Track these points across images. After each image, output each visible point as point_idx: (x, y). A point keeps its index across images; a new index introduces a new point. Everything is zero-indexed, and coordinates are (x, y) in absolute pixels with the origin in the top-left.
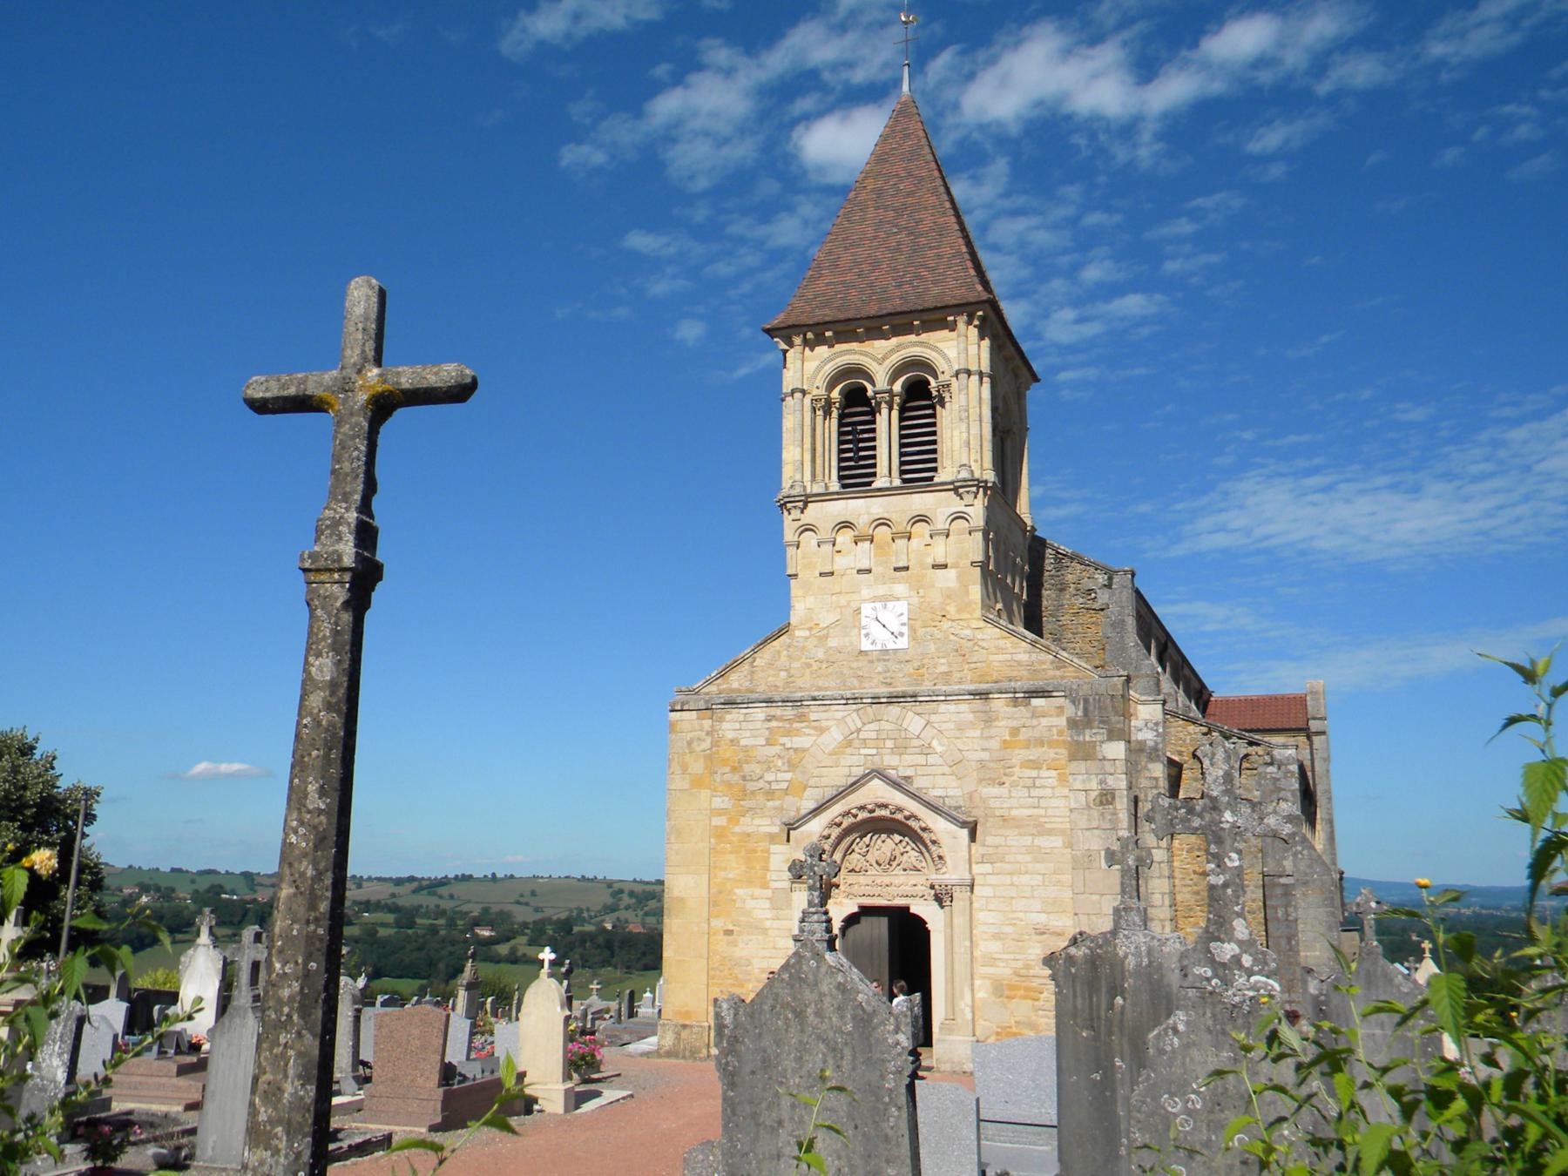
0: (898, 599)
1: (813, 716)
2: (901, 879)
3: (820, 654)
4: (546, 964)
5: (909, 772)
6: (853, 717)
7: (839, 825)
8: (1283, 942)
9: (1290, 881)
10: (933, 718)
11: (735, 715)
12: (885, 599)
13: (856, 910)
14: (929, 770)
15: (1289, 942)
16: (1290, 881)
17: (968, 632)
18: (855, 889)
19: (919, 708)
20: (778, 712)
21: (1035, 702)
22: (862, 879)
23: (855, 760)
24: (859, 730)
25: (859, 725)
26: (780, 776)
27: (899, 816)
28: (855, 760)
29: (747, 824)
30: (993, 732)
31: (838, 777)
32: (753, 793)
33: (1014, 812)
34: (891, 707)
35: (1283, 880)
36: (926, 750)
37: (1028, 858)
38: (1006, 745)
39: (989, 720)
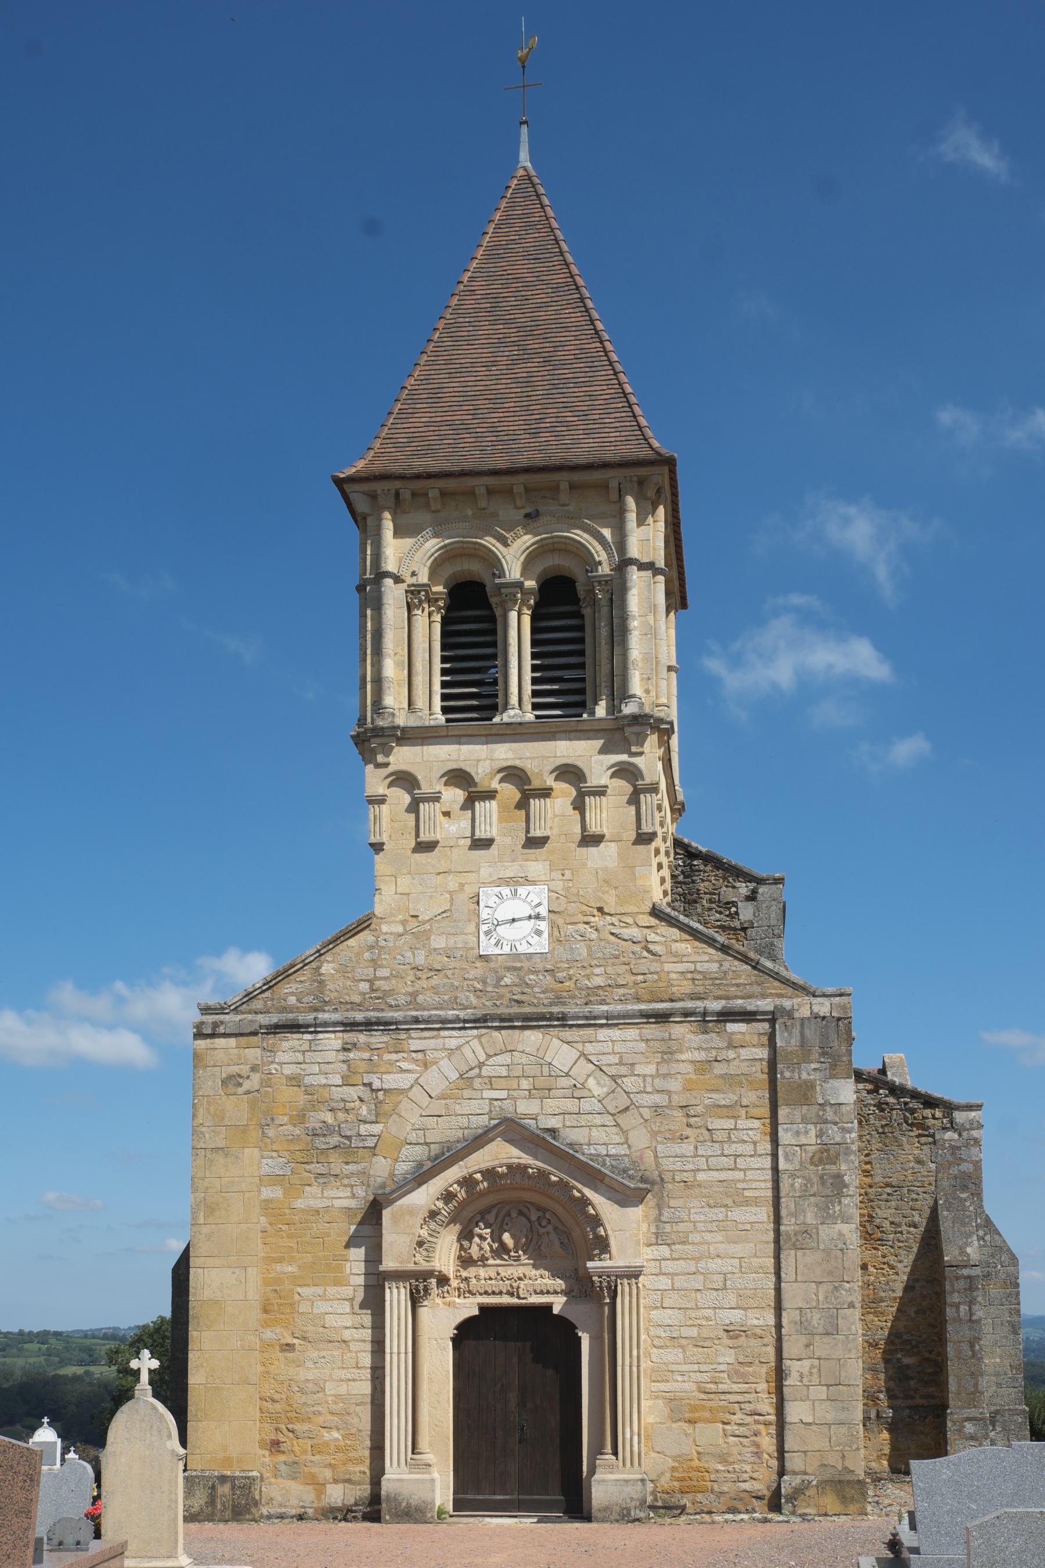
0: (533, 883)
1: (415, 1045)
3: (421, 959)
4: (145, 1377)
5: (553, 1123)
6: (473, 1045)
8: (965, 1347)
9: (977, 1271)
10: (589, 1048)
11: (294, 1041)
12: (513, 882)
13: (476, 1312)
14: (583, 1120)
15: (972, 1346)
16: (977, 1271)
17: (634, 932)
19: (568, 1034)
20: (362, 1038)
21: (731, 1027)
22: (482, 1272)
23: (474, 1106)
24: (481, 1065)
25: (482, 1057)
26: (364, 1129)
28: (474, 1106)
29: (313, 1197)
30: (675, 1067)
31: (447, 1130)
32: (324, 1152)
33: (701, 1176)
34: (527, 1033)
35: (965, 1272)
36: (577, 1091)
37: (719, 1237)
38: (688, 1088)
39: (668, 1053)
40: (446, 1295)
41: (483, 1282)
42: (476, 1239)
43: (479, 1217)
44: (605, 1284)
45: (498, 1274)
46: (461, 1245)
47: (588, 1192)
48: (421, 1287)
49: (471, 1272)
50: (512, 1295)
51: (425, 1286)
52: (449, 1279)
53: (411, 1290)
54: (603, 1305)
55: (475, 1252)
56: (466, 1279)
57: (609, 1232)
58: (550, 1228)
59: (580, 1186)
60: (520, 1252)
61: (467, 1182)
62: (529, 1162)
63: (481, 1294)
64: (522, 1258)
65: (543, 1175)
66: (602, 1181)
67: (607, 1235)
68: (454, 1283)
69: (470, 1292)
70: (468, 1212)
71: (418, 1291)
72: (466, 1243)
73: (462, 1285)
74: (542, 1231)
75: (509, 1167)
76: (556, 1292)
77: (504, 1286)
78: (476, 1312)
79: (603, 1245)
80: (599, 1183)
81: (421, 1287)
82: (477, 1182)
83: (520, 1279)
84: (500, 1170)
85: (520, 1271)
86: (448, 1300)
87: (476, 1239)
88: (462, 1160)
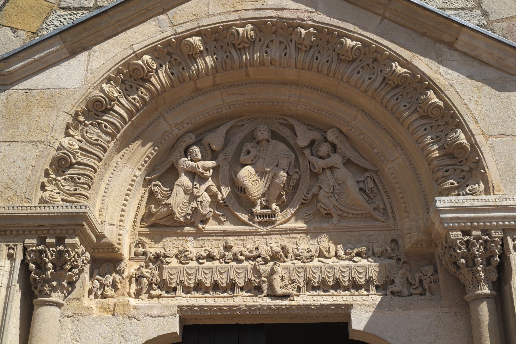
41: (194, 263)
42: (184, 180)
43: (191, 138)
44: (478, 249)
45: (228, 248)
46: (152, 193)
47: (425, 65)
49: (170, 245)
50: (257, 290)
51: (60, 254)
52: (119, 260)
53: (24, 264)
54: (466, 307)
55: (178, 201)
56: (158, 259)
57: (479, 139)
58: (336, 159)
59: (406, 54)
60: (274, 206)
61: (172, 52)
62: (301, 15)
64: (280, 218)
65: (328, 37)
66: (451, 45)
67: (474, 145)
69: (164, 285)
70: (173, 123)
71: (41, 267)
72: (158, 188)
74: (320, 163)
75: (260, 25)
76: (355, 286)
77: (242, 271)
78: (173, 326)
79: (465, 166)
80: (446, 49)
81: (49, 256)
82: (193, 55)
84: (240, 30)
85: (275, 243)
87: (184, 180)
88: (164, 11)
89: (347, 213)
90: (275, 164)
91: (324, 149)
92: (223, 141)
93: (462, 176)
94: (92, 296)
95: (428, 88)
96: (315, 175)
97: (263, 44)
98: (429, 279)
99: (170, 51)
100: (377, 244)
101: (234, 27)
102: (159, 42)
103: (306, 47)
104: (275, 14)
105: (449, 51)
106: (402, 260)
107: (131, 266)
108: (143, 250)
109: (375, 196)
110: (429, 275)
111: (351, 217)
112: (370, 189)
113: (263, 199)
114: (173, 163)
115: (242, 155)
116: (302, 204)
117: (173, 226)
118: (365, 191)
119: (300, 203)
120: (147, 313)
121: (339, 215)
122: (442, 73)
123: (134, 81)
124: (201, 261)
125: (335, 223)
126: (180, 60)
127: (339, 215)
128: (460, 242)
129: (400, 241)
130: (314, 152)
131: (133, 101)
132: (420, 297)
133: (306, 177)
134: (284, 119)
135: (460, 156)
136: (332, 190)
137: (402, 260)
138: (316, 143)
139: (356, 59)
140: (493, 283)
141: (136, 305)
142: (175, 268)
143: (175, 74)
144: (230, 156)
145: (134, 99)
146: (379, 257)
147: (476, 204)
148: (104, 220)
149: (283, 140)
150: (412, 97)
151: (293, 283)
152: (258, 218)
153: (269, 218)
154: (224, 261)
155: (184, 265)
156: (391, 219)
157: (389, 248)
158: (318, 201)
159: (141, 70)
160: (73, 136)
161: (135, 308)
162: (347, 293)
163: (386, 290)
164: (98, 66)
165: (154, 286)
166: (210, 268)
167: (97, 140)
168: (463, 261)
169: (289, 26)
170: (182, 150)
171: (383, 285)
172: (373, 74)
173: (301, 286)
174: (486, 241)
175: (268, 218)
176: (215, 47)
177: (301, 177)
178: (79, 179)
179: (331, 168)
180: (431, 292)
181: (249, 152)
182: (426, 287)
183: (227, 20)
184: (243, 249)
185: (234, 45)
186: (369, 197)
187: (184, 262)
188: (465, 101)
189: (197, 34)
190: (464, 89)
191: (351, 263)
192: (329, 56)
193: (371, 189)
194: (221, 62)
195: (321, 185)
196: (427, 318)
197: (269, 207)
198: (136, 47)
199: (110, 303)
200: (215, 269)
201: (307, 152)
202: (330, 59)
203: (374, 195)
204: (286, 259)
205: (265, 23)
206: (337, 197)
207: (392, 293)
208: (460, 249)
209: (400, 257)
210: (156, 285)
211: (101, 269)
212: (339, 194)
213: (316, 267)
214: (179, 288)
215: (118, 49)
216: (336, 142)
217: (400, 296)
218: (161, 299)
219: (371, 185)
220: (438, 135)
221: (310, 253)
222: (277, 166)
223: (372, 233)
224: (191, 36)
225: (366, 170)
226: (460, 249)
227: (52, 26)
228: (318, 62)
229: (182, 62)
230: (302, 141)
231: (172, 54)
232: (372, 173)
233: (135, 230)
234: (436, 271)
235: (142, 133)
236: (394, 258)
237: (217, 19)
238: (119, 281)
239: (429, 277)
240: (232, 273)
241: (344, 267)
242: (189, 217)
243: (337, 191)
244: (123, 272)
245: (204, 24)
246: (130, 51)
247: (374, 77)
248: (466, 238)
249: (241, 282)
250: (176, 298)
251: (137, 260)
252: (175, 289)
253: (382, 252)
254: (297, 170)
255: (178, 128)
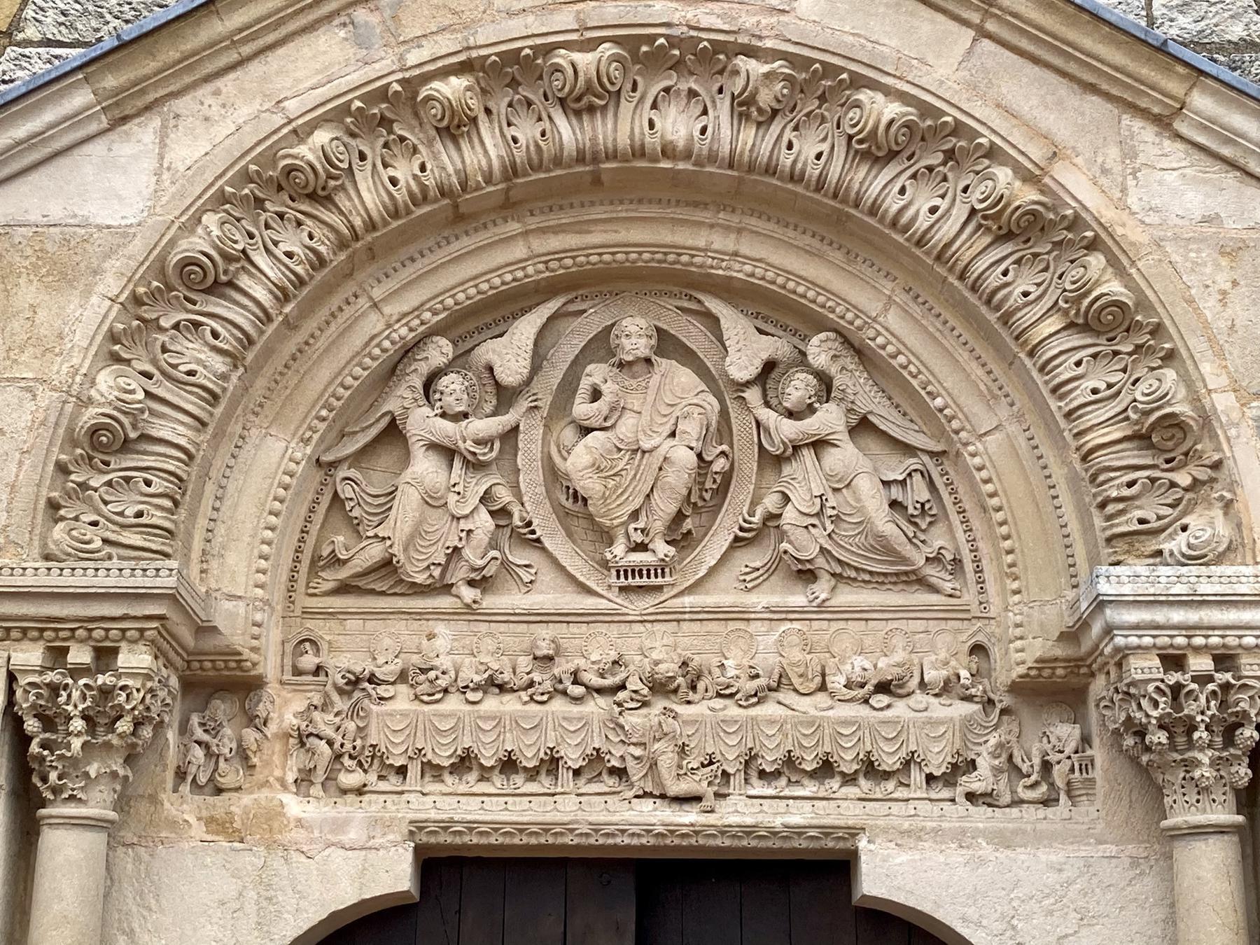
2: (767, 648)
7: (318, 191)
13: (395, 875)
18: (395, 717)
22: (447, 645)
27: (808, 148)
40: (230, 775)
44: (1200, 707)
48: (75, 702)
58: (829, 419)
63: (432, 770)
66: (1163, 123)
68: (285, 708)
73: (324, 723)
74: (788, 429)
80: (1146, 133)
83: (661, 687)
86: (240, 804)
89: (857, 569)
90: (667, 430)
91: (798, 388)
92: (527, 363)
93: (1169, 501)
94: (185, 788)
95: (1093, 245)
96: (774, 461)
97: (642, 99)
98: (1069, 762)
99: (388, 114)
100: (933, 658)
101: (563, 51)
102: (358, 93)
103: (760, 110)
104: (677, 15)
105: (1157, 140)
106: (999, 706)
107: (286, 702)
108: (317, 660)
109: (931, 523)
110: (1068, 751)
111: (864, 581)
112: (918, 506)
113: (633, 526)
114: (394, 420)
115: (577, 401)
116: (737, 539)
117: (395, 594)
118: (906, 508)
119: (732, 537)
120: (333, 839)
121: (834, 575)
122: (1135, 208)
123: (290, 202)
124: (471, 696)
125: (823, 596)
126: (416, 142)
127: (834, 575)
128: (1157, 688)
129: (996, 652)
130: (771, 394)
131: (286, 260)
132: (1042, 812)
133: (748, 463)
134: (691, 298)
135: (1170, 444)
136: (817, 508)
137: (999, 706)
138: (777, 370)
139: (898, 152)
140: (1237, 792)
141: (303, 815)
142: (404, 714)
143: (402, 183)
144: (546, 402)
145: (290, 255)
146: (936, 695)
147: (1205, 588)
148: (213, 586)
149: (687, 356)
150: (1046, 269)
151: (711, 763)
152: (618, 577)
153: (649, 577)
154: (532, 699)
155: (426, 708)
156: (973, 588)
157: (964, 674)
158: (782, 536)
159: (311, 176)
160: (128, 362)
161: (300, 823)
162: (851, 791)
163: (954, 785)
164: (188, 163)
165: (346, 761)
166: (494, 718)
167: (191, 373)
168: (1162, 737)
169: (718, 47)
170: (418, 383)
171: (944, 773)
172: (943, 197)
173: (731, 771)
174: (1226, 687)
175: (645, 579)
176: (510, 105)
177: (736, 464)
178: (148, 483)
179: (819, 445)
180: (1070, 797)
181: (596, 395)
182: (1060, 783)
183: (545, 30)
184: (581, 663)
185: (562, 102)
186: (916, 524)
187: (426, 698)
188: (1193, 291)
189: (464, 68)
190: (1193, 255)
191: (863, 711)
192: (824, 139)
193: (923, 505)
194: (528, 147)
195: (787, 492)
196: (1060, 870)
197: (650, 546)
198: (293, 107)
199: (232, 808)
200: (508, 717)
201: (753, 395)
202: (825, 147)
203: (928, 519)
204: (691, 696)
205: (651, 39)
206: (830, 527)
207: (971, 797)
208: (1156, 704)
209: (992, 696)
210: (351, 757)
211: (207, 712)
212: (836, 519)
213: (772, 722)
214: (414, 770)
215: (245, 111)
216: (833, 370)
217: (990, 805)
218: (366, 798)
219: (925, 495)
220: (1113, 380)
221: (757, 682)
222: (673, 434)
223: (920, 625)
224: (444, 73)
225: (909, 450)
226: (1156, 704)
227: (50, 13)
228: (792, 158)
229: (420, 147)
230: (742, 366)
231: (392, 122)
232: (926, 458)
233: (293, 602)
234: (1086, 740)
235: (312, 341)
236: (976, 699)
237: (515, 27)
238: (254, 748)
239: (1069, 758)
240: (551, 734)
241: (846, 723)
242: (437, 572)
243: (830, 512)
244: (265, 724)
245: (481, 42)
246: (279, 120)
247: (944, 205)
248: (1174, 678)
249: (573, 756)
250: (405, 797)
251: (298, 688)
252: (402, 771)
253: (947, 682)
254: (725, 447)
255: (406, 324)
